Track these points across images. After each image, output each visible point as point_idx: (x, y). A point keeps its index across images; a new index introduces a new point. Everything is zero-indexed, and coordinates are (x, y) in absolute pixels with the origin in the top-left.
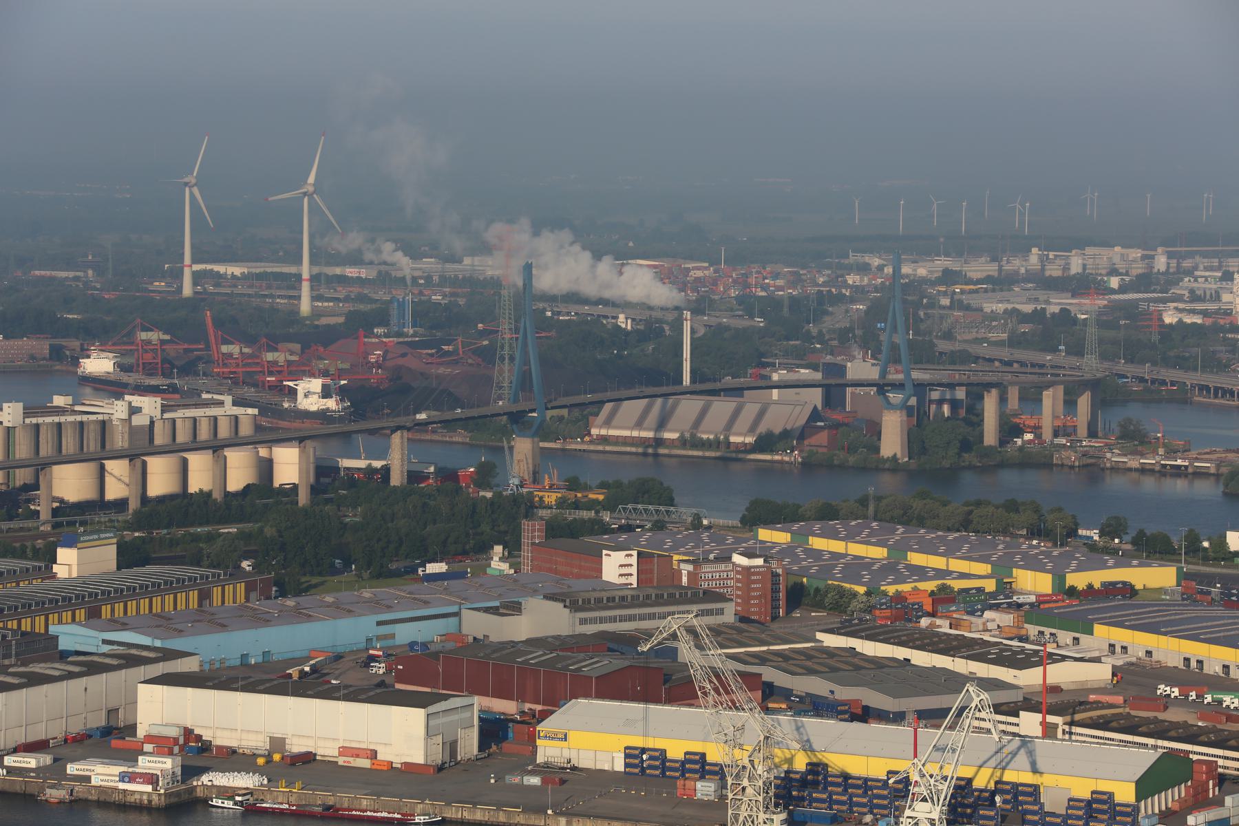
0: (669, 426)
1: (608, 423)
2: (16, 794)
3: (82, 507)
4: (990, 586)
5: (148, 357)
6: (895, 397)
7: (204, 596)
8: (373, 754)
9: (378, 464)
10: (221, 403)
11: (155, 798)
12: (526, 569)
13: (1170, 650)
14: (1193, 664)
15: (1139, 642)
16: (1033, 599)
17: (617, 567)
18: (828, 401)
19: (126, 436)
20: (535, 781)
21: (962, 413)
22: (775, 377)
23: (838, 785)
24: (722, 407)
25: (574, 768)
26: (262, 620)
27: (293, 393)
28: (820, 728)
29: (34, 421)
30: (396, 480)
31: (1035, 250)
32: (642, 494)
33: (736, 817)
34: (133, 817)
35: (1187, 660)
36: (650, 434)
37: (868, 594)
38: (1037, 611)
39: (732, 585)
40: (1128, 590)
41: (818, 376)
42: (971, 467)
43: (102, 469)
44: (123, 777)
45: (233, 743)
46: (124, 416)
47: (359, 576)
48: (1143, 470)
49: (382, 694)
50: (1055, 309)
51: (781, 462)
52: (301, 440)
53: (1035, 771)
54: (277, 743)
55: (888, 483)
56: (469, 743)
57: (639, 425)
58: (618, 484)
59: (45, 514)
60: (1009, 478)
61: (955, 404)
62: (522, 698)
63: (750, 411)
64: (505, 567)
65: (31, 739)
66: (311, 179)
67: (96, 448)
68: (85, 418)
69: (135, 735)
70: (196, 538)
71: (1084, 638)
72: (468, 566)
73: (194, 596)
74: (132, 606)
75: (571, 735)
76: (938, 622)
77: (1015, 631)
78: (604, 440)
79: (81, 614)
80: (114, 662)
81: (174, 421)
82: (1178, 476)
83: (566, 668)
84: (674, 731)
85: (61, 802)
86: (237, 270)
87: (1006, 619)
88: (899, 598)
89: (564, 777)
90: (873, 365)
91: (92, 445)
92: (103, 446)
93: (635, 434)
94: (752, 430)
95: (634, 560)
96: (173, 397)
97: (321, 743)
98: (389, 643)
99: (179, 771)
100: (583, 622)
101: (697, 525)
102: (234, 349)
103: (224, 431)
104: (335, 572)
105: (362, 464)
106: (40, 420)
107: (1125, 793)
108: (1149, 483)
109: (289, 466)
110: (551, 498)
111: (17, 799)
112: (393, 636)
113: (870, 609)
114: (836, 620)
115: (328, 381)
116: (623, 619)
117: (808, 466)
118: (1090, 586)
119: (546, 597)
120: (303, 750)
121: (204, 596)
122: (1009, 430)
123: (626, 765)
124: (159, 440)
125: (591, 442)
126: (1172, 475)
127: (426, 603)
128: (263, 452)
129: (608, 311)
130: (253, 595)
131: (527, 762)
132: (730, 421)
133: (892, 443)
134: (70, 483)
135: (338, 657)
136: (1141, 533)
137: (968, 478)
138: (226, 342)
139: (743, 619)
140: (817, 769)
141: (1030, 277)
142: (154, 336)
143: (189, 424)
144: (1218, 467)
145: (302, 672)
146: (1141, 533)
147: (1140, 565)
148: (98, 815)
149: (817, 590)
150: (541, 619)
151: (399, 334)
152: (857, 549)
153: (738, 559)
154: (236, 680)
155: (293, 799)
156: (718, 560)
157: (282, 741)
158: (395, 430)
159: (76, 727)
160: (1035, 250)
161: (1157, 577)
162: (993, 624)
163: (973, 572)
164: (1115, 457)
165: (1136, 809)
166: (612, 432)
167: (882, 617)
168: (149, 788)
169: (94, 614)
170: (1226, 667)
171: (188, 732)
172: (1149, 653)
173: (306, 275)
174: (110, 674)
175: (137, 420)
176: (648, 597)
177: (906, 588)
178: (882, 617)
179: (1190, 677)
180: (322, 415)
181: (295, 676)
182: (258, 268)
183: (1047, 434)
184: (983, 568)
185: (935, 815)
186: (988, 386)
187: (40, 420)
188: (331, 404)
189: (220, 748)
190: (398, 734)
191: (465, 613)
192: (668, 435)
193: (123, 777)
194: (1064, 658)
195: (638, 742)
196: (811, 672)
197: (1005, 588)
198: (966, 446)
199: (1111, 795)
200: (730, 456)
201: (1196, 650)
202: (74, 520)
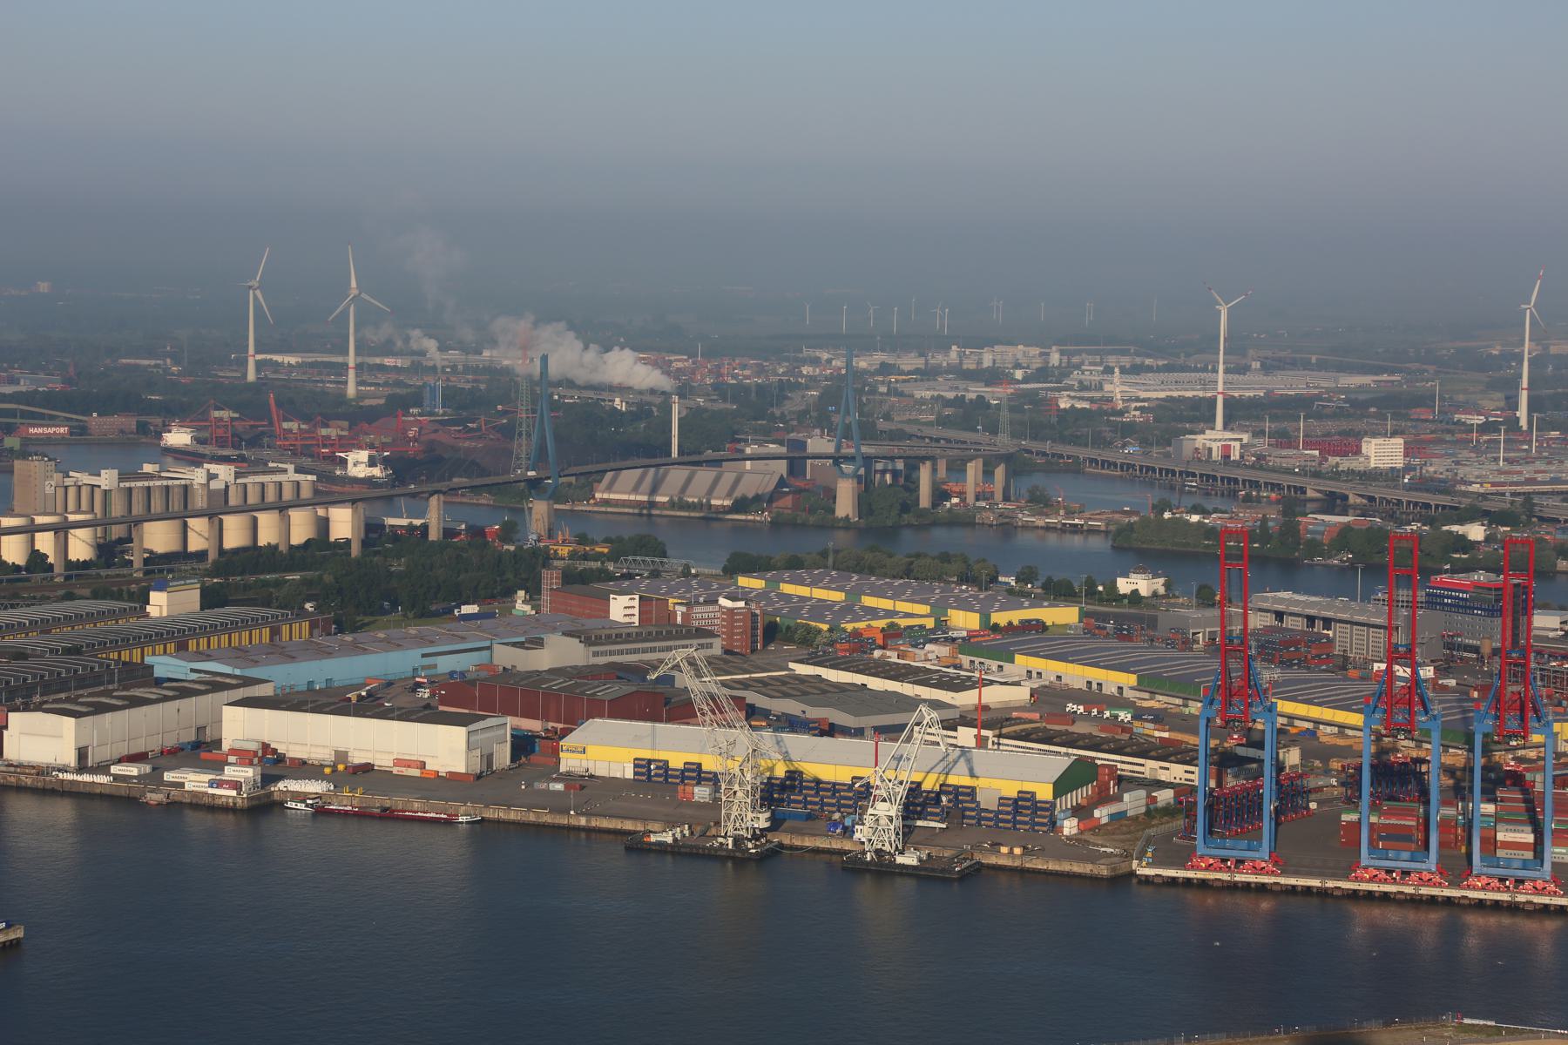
0: (661, 490)
1: (609, 489)
2: (121, 797)
3: (168, 557)
4: (930, 623)
5: (220, 432)
6: (847, 468)
7: (275, 632)
8: (423, 765)
9: (417, 522)
10: (285, 471)
11: (239, 801)
12: (546, 610)
13: (1076, 675)
14: (1094, 686)
15: (1051, 669)
16: (964, 634)
17: (622, 608)
18: (792, 470)
20: (559, 787)
21: (902, 481)
22: (748, 451)
23: (810, 788)
24: (704, 476)
25: (591, 776)
26: (328, 653)
27: (344, 462)
28: (797, 743)
29: (127, 485)
30: (433, 535)
31: (954, 348)
32: (640, 547)
33: (728, 816)
34: (221, 817)
35: (1089, 683)
36: (645, 498)
37: (830, 630)
38: (968, 644)
39: (718, 624)
40: (1040, 626)
41: (784, 450)
42: (909, 526)
43: (185, 525)
44: (211, 784)
45: (304, 756)
46: (204, 481)
47: (405, 616)
49: (427, 714)
50: (973, 396)
52: (354, 502)
53: (972, 775)
54: (341, 756)
55: (841, 539)
56: (503, 756)
57: (635, 490)
58: (620, 540)
59: (138, 563)
60: (940, 534)
61: (895, 474)
62: (546, 718)
63: (728, 478)
64: (527, 608)
65: (134, 751)
66: (354, 284)
67: (180, 508)
68: (170, 483)
69: (220, 748)
70: (266, 584)
71: (1006, 665)
72: (496, 607)
73: (266, 632)
74: (214, 640)
75: (589, 749)
76: (888, 653)
77: (951, 661)
78: (607, 502)
79: (171, 647)
80: (202, 687)
81: (245, 485)
82: (1075, 532)
83: (583, 693)
84: (676, 746)
85: (159, 804)
86: (292, 359)
87: (943, 651)
88: (856, 633)
89: (583, 783)
91: (176, 505)
92: (186, 506)
93: (632, 497)
94: (729, 495)
95: (636, 603)
96: (245, 465)
97: (378, 756)
98: (432, 672)
99: (259, 778)
100: (596, 654)
101: (686, 573)
102: (293, 426)
103: (288, 495)
104: (384, 612)
105: (404, 522)
106: (133, 484)
107: (1045, 792)
108: (1052, 539)
109: (343, 523)
110: (564, 551)
111: (123, 800)
112: (435, 666)
113: (832, 643)
114: (804, 653)
115: (374, 453)
116: (629, 652)
117: (776, 524)
118: (1010, 623)
119: (564, 634)
120: (363, 761)
121: (275, 632)
122: (940, 495)
123: (636, 773)
124: (233, 501)
125: (596, 504)
127: (463, 639)
128: (321, 512)
129: (605, 395)
130: (316, 632)
131: (551, 770)
132: (710, 487)
133: (845, 505)
134: (158, 537)
135: (390, 684)
136: (1049, 580)
137: (907, 534)
138: (286, 420)
139: (727, 652)
140: (794, 775)
141: (951, 369)
142: (225, 414)
143: (258, 488)
144: (1107, 525)
145: (360, 698)
146: (1049, 580)
147: (1050, 606)
148: (191, 817)
149: (788, 628)
150: (560, 652)
151: (431, 414)
152: (819, 593)
153: (723, 602)
154: (306, 703)
155: (355, 802)
156: (706, 602)
157: (346, 753)
158: (432, 494)
159: (171, 742)
160: (954, 348)
161: (1064, 615)
162: (932, 655)
163: (914, 612)
164: (1025, 518)
165: (1053, 805)
166: (612, 496)
167: (841, 650)
168: (234, 793)
169: (182, 647)
170: (1120, 689)
171: (265, 746)
172: (1059, 678)
173: (351, 364)
174: (200, 698)
175: (216, 485)
176: (650, 633)
177: (861, 625)
178: (841, 650)
179: (1092, 696)
180: (369, 481)
181: (354, 700)
182: (311, 358)
183: (970, 499)
184: (924, 609)
185: (893, 813)
186: (923, 459)
187: (133, 484)
188: (376, 471)
189: (292, 759)
190: (444, 748)
191: (496, 647)
192: (659, 499)
193: (211, 784)
194: (992, 682)
195: (647, 754)
196: (786, 695)
197: (942, 625)
198: (905, 508)
199: (1033, 794)
200: (711, 517)
201: (1096, 674)
202: (163, 569)
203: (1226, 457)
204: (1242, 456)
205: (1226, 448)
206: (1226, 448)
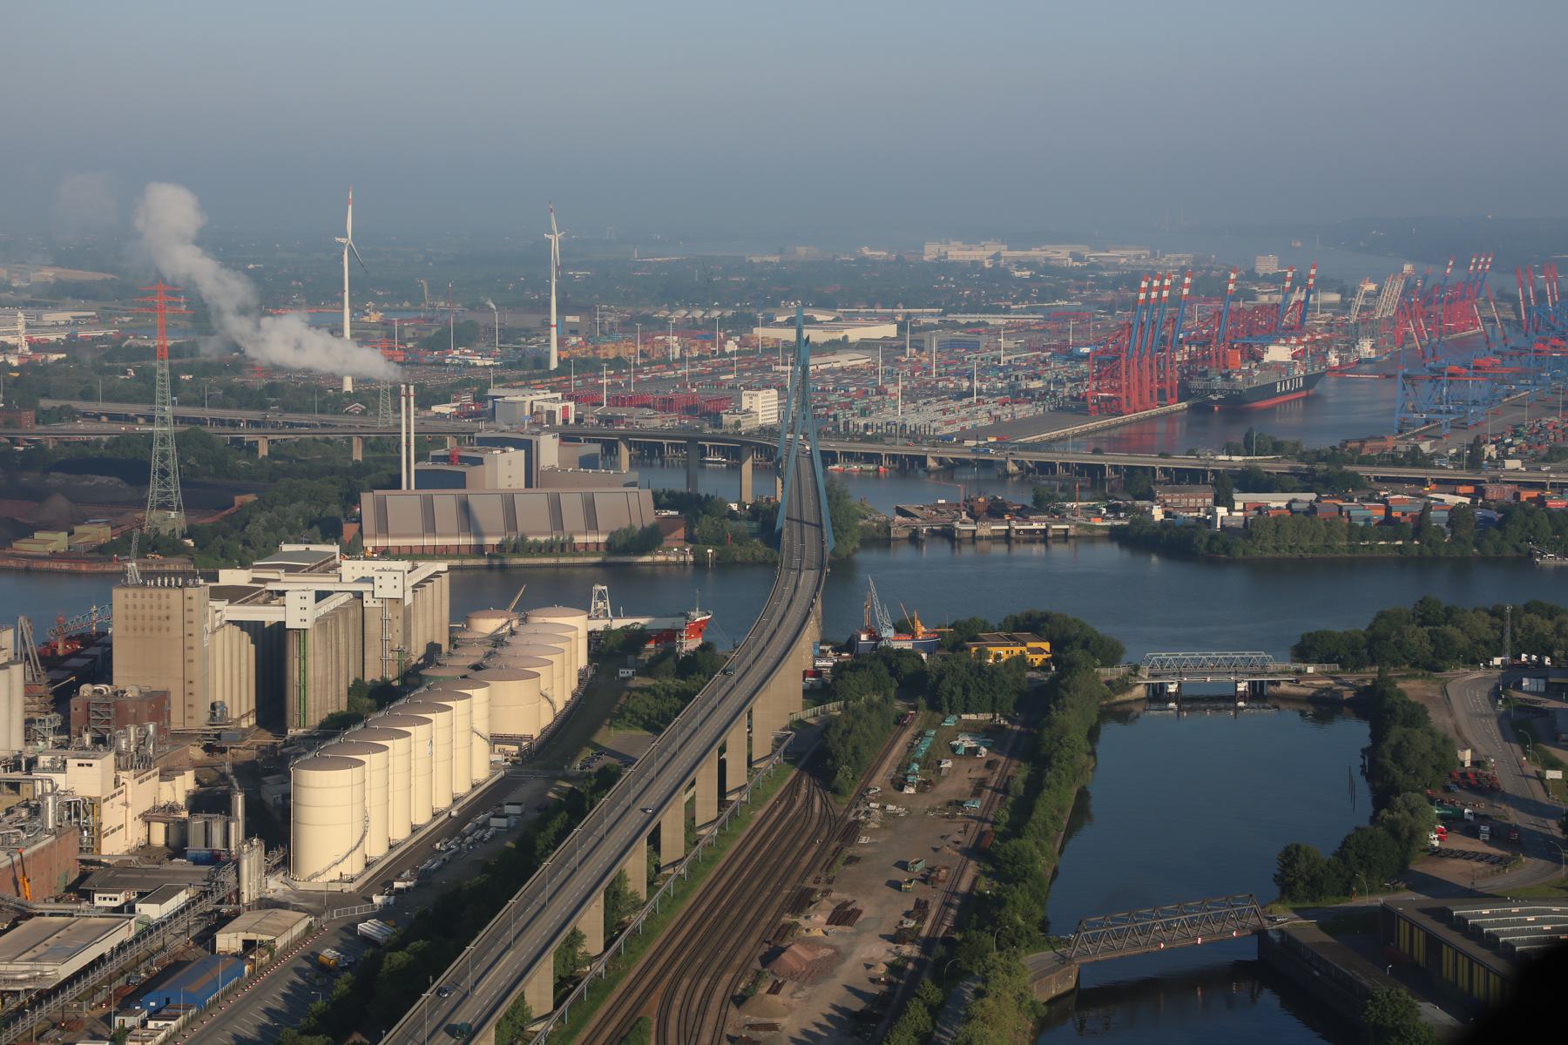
1: (383, 529)
19: (398, 624)
48: (993, 539)
51: (666, 564)
57: (430, 528)
94: (592, 525)
108: (1000, 549)
126: (1026, 542)
166: (391, 542)
203: (566, 421)
204: (579, 420)
205: (565, 409)
206: (565, 409)
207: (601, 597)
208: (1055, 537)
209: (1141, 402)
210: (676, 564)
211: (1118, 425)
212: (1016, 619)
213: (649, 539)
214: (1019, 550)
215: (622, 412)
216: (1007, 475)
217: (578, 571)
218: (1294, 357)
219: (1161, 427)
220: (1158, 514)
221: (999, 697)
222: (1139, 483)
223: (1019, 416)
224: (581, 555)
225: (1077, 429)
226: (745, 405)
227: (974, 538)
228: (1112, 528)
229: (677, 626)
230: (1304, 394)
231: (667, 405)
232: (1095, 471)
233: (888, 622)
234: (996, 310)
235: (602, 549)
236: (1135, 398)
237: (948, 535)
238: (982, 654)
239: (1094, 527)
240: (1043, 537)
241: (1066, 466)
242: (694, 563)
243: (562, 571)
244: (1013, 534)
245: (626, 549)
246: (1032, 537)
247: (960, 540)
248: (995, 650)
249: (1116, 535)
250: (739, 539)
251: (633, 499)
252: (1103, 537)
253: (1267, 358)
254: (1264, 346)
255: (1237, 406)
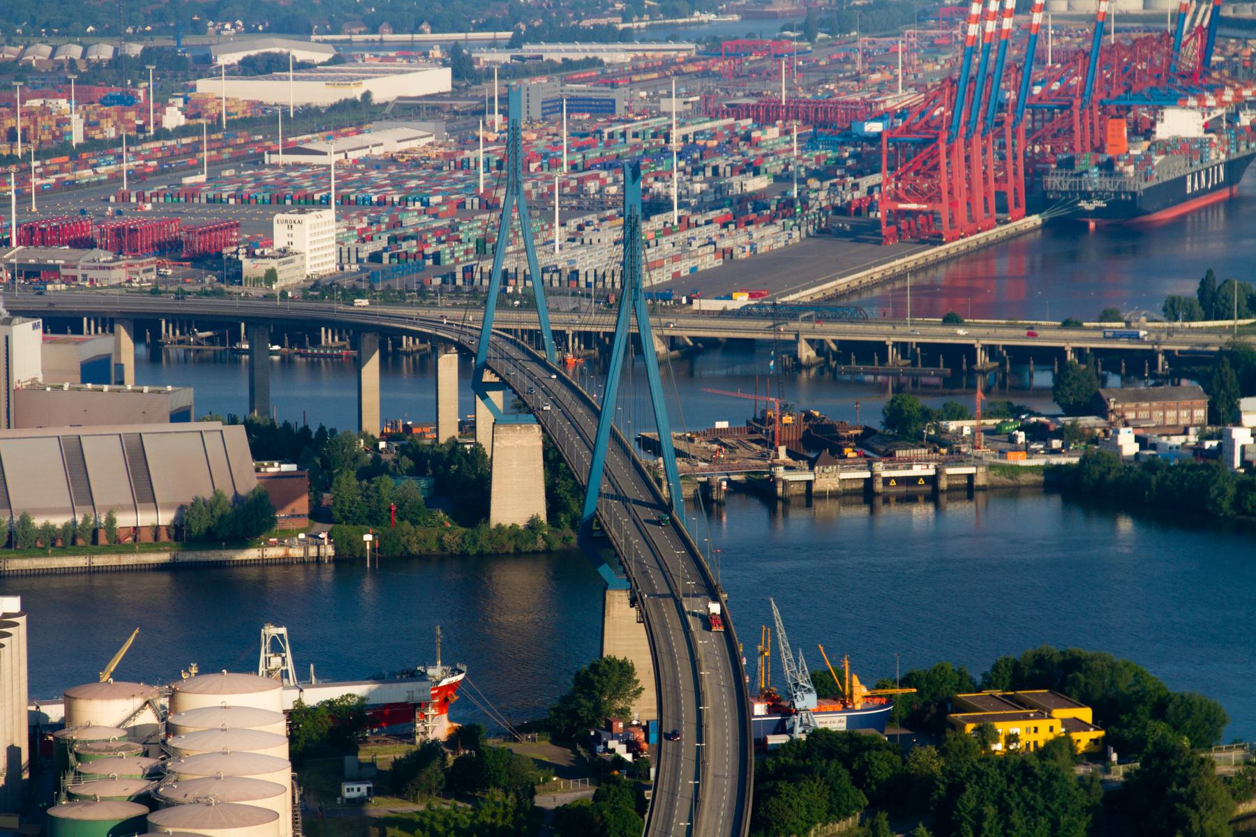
48: (843, 496)
51: (286, 562)
82: (911, 499)
90: (35, 327)
94: (144, 494)
207: (276, 647)
208: (951, 489)
209: (972, 219)
210: (302, 562)
211: (938, 263)
212: (1016, 666)
213: (250, 518)
214: (891, 514)
215: (58, 256)
216: (799, 366)
217: (125, 581)
218: (1208, 128)
219: (1001, 266)
220: (1128, 444)
221: (1064, 819)
222: (1083, 385)
223: (762, 248)
224: (130, 550)
225: (876, 272)
226: (280, 241)
227: (810, 495)
228: (1049, 470)
229: (418, 697)
230: (1225, 193)
231: (123, 241)
232: (958, 358)
233: (804, 680)
234: (606, 35)
235: (164, 537)
236: (962, 213)
237: (761, 490)
238: (986, 734)
239: (1016, 470)
240: (932, 491)
241: (902, 347)
242: (336, 560)
243: (99, 581)
244: (879, 487)
245: (211, 539)
246: (910, 491)
247: (786, 501)
248: (1003, 728)
249: (1054, 480)
250: (406, 512)
251: (213, 442)
252: (1035, 486)
253: (1163, 132)
254: (1157, 110)
255: (1128, 223)
